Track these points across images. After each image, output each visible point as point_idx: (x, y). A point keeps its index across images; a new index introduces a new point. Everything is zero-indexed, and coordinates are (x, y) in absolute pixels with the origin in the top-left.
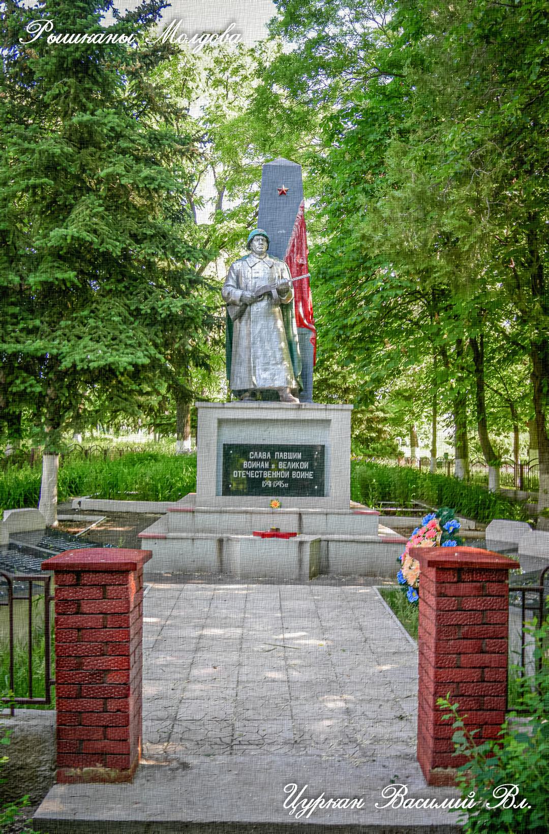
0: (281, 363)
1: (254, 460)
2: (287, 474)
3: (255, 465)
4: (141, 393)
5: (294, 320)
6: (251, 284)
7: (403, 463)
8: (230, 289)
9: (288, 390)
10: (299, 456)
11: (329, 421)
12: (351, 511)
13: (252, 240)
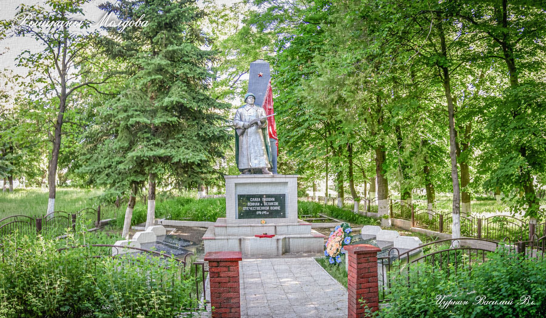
0: (263, 156)
1: (252, 202)
2: (268, 208)
3: (253, 204)
4: (202, 173)
5: (268, 136)
6: (247, 118)
7: (310, 200)
8: (237, 121)
9: (267, 169)
10: (274, 199)
11: (286, 183)
12: (298, 224)
13: (247, 98)
